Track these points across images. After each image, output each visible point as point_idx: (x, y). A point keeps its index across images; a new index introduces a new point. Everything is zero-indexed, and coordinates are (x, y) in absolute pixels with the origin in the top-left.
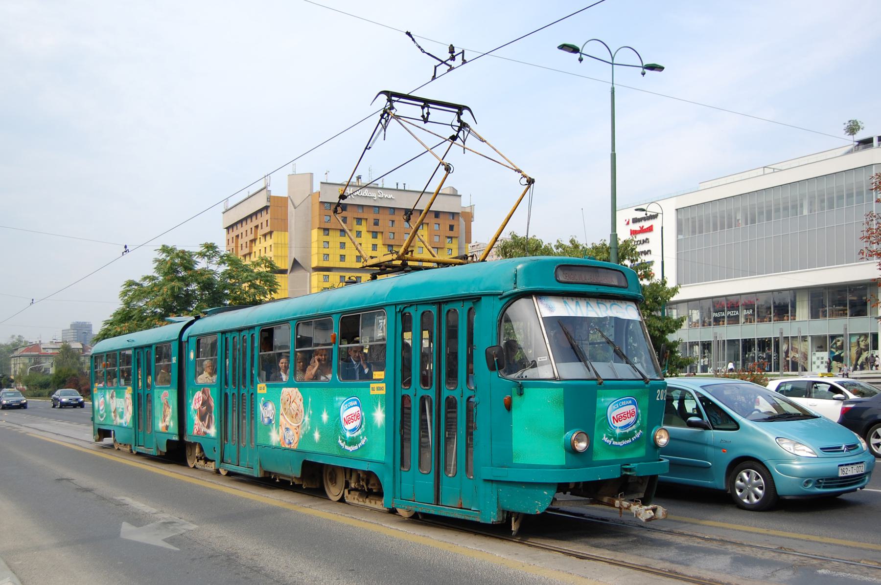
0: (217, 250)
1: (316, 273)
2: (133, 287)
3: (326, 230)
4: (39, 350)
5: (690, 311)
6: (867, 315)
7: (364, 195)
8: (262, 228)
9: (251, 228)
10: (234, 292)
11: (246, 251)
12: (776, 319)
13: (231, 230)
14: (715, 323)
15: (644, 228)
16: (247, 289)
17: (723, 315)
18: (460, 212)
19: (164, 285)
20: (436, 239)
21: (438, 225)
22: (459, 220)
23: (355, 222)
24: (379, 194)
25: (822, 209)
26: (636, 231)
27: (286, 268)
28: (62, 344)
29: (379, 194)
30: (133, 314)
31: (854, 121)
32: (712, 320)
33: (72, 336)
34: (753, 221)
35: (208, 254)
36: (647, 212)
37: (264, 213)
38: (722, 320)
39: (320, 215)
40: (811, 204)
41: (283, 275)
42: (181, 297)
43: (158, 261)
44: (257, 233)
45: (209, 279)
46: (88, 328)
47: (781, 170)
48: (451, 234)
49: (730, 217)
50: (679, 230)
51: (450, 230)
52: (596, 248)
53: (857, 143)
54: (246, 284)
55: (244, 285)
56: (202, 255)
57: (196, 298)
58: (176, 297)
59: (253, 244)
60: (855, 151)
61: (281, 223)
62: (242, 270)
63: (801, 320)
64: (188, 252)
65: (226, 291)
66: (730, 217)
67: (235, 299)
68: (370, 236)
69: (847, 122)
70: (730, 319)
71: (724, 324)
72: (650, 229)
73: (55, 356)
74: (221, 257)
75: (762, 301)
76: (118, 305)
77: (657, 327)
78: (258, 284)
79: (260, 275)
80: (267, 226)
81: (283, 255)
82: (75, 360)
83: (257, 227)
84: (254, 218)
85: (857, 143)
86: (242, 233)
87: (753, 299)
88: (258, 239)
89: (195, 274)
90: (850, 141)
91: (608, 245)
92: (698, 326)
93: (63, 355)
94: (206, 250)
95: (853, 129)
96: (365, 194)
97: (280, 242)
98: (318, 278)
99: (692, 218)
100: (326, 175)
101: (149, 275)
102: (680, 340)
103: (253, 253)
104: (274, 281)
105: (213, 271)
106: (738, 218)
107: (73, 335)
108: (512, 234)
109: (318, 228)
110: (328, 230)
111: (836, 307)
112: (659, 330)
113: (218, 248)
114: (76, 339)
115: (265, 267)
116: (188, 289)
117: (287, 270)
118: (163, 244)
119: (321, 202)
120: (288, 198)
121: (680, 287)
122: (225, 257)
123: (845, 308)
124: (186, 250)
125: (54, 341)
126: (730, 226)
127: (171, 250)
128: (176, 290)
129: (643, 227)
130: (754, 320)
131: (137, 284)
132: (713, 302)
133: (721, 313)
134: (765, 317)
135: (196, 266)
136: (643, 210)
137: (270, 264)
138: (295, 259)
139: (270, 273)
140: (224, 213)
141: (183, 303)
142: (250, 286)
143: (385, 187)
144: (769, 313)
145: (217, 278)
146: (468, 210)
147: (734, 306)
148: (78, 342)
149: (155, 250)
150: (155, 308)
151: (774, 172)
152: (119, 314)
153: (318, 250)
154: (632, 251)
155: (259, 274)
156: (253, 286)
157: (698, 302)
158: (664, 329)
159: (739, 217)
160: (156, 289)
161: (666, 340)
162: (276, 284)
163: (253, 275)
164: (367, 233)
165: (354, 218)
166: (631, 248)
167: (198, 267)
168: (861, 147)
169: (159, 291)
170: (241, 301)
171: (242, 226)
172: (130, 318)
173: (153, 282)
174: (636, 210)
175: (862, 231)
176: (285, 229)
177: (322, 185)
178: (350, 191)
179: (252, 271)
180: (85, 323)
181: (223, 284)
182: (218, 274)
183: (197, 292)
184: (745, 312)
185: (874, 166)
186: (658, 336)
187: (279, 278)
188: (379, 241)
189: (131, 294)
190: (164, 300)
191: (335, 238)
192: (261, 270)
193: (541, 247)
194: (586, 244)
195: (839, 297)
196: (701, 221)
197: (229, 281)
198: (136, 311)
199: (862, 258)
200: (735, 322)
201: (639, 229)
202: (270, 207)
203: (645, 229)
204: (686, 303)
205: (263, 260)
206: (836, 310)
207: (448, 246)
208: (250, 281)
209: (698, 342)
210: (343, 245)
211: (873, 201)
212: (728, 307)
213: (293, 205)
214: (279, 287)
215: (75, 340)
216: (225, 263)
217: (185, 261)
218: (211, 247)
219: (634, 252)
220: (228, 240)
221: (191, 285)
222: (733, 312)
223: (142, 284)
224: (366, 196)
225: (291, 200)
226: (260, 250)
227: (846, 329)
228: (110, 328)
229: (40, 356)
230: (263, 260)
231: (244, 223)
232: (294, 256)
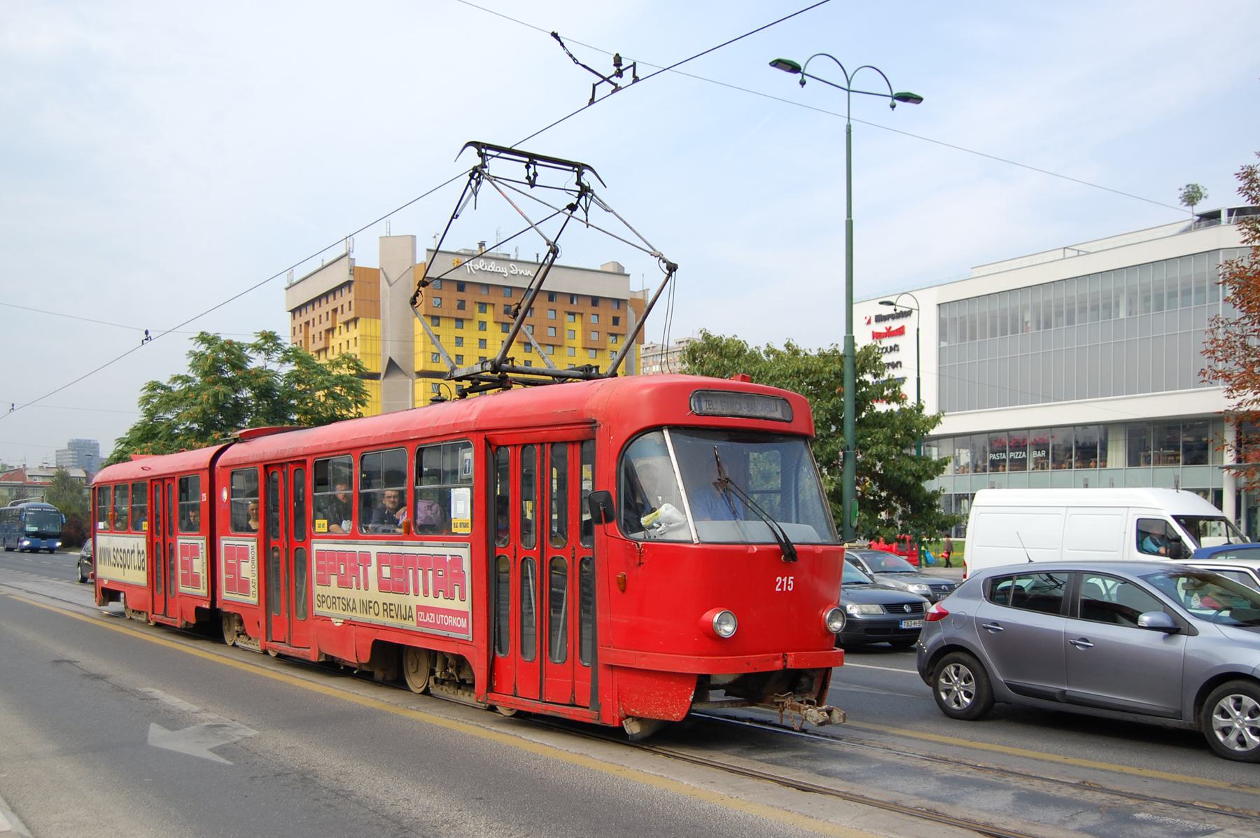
0: (279, 342)
1: (421, 380)
2: (158, 391)
3: (436, 319)
4: (24, 478)
5: (957, 450)
6: (1207, 464)
7: (489, 270)
8: (342, 313)
9: (327, 313)
10: (304, 403)
11: (321, 345)
12: (1078, 465)
13: (297, 315)
14: (991, 469)
15: (892, 330)
16: (323, 399)
17: (1004, 457)
18: (628, 298)
19: (203, 389)
20: (594, 336)
21: (596, 316)
22: (626, 310)
23: (477, 308)
24: (511, 269)
25: (1147, 310)
26: (880, 333)
27: (378, 371)
28: (57, 470)
29: (511, 269)
30: (158, 430)
31: (1193, 185)
32: (988, 464)
33: (71, 460)
34: (1048, 325)
35: (266, 347)
36: (897, 307)
37: (345, 291)
38: (1002, 464)
40: (1131, 302)
41: (373, 381)
42: (228, 408)
43: (195, 354)
44: (336, 320)
45: (267, 382)
46: (94, 448)
47: (1088, 253)
48: (615, 329)
49: (1014, 319)
50: (942, 335)
51: (614, 324)
52: (823, 356)
53: (1198, 218)
54: (321, 393)
55: (318, 393)
56: (257, 348)
57: (249, 409)
58: (220, 408)
59: (331, 336)
60: (1195, 229)
61: (370, 307)
62: (316, 372)
63: (1114, 467)
64: (238, 343)
65: (292, 402)
66: (1014, 319)
67: (306, 413)
68: (499, 328)
69: (1185, 187)
70: (1013, 463)
71: (1004, 470)
72: (900, 332)
73: (47, 487)
74: (285, 352)
75: (1059, 439)
76: (136, 416)
77: (911, 470)
78: (339, 392)
79: (342, 380)
80: (350, 309)
81: (374, 351)
82: (75, 494)
83: (335, 311)
84: (331, 298)
85: (1198, 218)
86: (314, 319)
87: (1046, 435)
88: (338, 329)
89: (247, 375)
90: (1189, 214)
91: (841, 352)
92: (968, 472)
93: (58, 485)
94: (263, 341)
95: (1192, 197)
97: (368, 333)
98: (425, 388)
99: (961, 318)
101: (182, 374)
102: (940, 490)
103: (331, 348)
104: (362, 389)
105: (273, 371)
106: (1026, 320)
107: (72, 458)
108: (703, 332)
110: (438, 318)
111: (1165, 451)
112: (913, 475)
113: (280, 339)
114: (76, 464)
115: (348, 368)
116: (237, 397)
117: (379, 374)
118: (202, 331)
120: (379, 270)
121: (944, 415)
122: (290, 352)
123: (1176, 453)
124: (235, 340)
125: (45, 466)
126: (1014, 331)
127: (213, 339)
128: (221, 397)
129: (890, 328)
130: (1048, 466)
131: (164, 388)
132: (989, 438)
133: (1001, 454)
134: (1063, 462)
135: (249, 363)
136: (891, 304)
137: (355, 363)
138: (390, 359)
139: (356, 377)
140: (287, 289)
141: (231, 417)
142: (326, 396)
143: (519, 259)
144: (1068, 456)
145: (279, 381)
146: (640, 297)
147: (1019, 446)
148: (79, 468)
149: (192, 338)
150: (191, 423)
151: (1078, 255)
152: (138, 429)
153: (424, 347)
154: (875, 362)
155: (340, 377)
156: (331, 395)
157: (968, 437)
158: (921, 474)
159: (1028, 317)
160: (191, 395)
161: (923, 489)
162: (364, 393)
163: (332, 379)
165: (476, 302)
166: (874, 357)
167: (251, 366)
168: (1203, 223)
169: (196, 399)
170: (314, 416)
171: (314, 309)
172: (155, 435)
173: (188, 384)
174: (881, 303)
175: (1204, 343)
176: (377, 315)
179: (329, 374)
180: (89, 440)
181: (289, 392)
182: (281, 376)
183: (250, 401)
184: (1035, 454)
185: (1221, 252)
186: (912, 483)
187: (368, 385)
189: (155, 401)
190: (204, 411)
191: (447, 331)
192: (343, 372)
193: (745, 351)
194: (810, 350)
195: (1168, 436)
196: (973, 322)
197: (296, 387)
198: (164, 426)
199: (1203, 381)
200: (1020, 468)
201: (885, 331)
203: (893, 331)
204: (952, 439)
205: (344, 358)
206: (1163, 455)
208: (327, 388)
209: (968, 494)
210: (459, 341)
211: (1218, 300)
212: (1010, 447)
213: (388, 280)
214: (368, 398)
215: (75, 466)
216: (289, 361)
217: (233, 357)
218: (270, 336)
219: (878, 363)
220: (294, 328)
221: (242, 391)
222: (1017, 453)
223: (170, 388)
224: (493, 272)
225: (385, 274)
226: (340, 344)
227: (1178, 482)
228: (126, 449)
229: (25, 486)
230: (344, 358)
231: (317, 305)
232: (389, 354)
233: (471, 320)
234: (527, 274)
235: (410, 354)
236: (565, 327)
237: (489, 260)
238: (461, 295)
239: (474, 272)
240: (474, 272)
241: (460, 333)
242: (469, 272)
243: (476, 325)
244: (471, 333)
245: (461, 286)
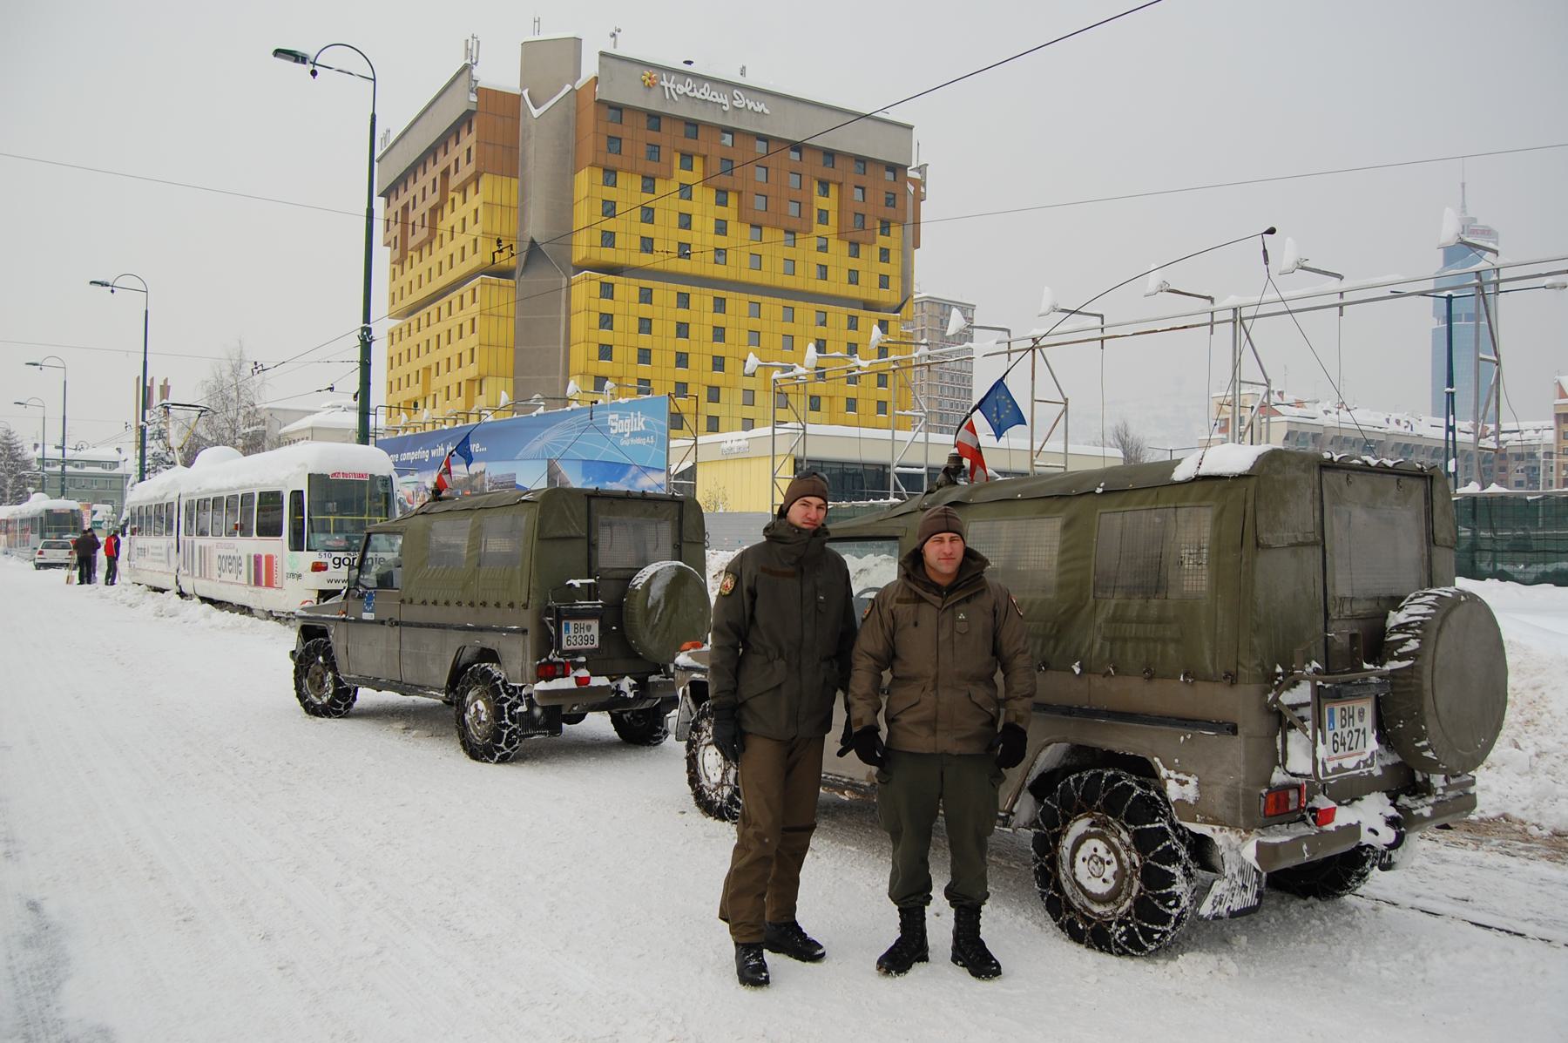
3: (610, 176)
7: (699, 96)
24: (735, 99)
29: (735, 99)
39: (596, 133)
97: (497, 200)
100: (613, 39)
119: (600, 102)
138: (533, 242)
177: (605, 60)
188: (730, 212)
207: (882, 241)
235: (564, 236)
236: (815, 205)
237: (700, 82)
238: (653, 137)
239: (676, 98)
240: (676, 98)
242: (668, 97)
245: (655, 119)
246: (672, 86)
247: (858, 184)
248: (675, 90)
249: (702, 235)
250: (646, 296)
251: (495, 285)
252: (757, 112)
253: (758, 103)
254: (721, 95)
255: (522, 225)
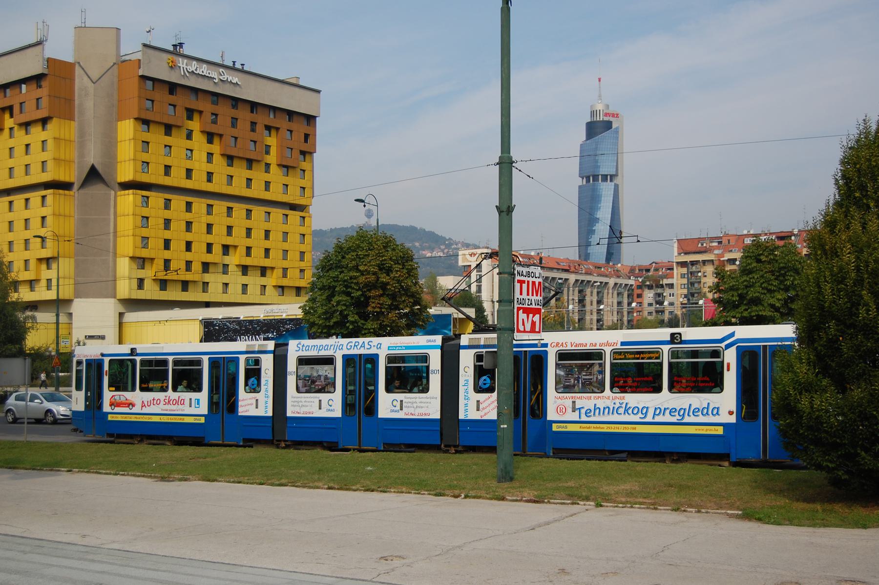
1: (123, 192)
7: (201, 73)
24: (221, 75)
27: (72, 180)
29: (221, 75)
41: (67, 192)
48: (305, 147)
68: (203, 139)
96: (203, 72)
97: (62, 137)
109: (136, 119)
153: (135, 155)
164: (200, 133)
177: (145, 49)
178: (183, 64)
188: (216, 148)
191: (157, 137)
202: (49, 77)
224: (205, 75)
233: (179, 127)
234: (234, 81)
237: (201, 64)
240: (188, 75)
241: (168, 140)
242: (183, 74)
243: (184, 133)
244: (177, 141)
246: (184, 66)
247: (289, 129)
248: (186, 69)
249: (200, 164)
250: (167, 204)
251: (62, 195)
252: (234, 83)
253: (234, 78)
254: (213, 72)
255: (81, 155)
